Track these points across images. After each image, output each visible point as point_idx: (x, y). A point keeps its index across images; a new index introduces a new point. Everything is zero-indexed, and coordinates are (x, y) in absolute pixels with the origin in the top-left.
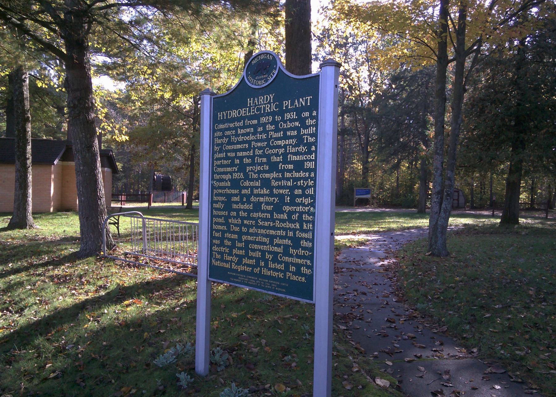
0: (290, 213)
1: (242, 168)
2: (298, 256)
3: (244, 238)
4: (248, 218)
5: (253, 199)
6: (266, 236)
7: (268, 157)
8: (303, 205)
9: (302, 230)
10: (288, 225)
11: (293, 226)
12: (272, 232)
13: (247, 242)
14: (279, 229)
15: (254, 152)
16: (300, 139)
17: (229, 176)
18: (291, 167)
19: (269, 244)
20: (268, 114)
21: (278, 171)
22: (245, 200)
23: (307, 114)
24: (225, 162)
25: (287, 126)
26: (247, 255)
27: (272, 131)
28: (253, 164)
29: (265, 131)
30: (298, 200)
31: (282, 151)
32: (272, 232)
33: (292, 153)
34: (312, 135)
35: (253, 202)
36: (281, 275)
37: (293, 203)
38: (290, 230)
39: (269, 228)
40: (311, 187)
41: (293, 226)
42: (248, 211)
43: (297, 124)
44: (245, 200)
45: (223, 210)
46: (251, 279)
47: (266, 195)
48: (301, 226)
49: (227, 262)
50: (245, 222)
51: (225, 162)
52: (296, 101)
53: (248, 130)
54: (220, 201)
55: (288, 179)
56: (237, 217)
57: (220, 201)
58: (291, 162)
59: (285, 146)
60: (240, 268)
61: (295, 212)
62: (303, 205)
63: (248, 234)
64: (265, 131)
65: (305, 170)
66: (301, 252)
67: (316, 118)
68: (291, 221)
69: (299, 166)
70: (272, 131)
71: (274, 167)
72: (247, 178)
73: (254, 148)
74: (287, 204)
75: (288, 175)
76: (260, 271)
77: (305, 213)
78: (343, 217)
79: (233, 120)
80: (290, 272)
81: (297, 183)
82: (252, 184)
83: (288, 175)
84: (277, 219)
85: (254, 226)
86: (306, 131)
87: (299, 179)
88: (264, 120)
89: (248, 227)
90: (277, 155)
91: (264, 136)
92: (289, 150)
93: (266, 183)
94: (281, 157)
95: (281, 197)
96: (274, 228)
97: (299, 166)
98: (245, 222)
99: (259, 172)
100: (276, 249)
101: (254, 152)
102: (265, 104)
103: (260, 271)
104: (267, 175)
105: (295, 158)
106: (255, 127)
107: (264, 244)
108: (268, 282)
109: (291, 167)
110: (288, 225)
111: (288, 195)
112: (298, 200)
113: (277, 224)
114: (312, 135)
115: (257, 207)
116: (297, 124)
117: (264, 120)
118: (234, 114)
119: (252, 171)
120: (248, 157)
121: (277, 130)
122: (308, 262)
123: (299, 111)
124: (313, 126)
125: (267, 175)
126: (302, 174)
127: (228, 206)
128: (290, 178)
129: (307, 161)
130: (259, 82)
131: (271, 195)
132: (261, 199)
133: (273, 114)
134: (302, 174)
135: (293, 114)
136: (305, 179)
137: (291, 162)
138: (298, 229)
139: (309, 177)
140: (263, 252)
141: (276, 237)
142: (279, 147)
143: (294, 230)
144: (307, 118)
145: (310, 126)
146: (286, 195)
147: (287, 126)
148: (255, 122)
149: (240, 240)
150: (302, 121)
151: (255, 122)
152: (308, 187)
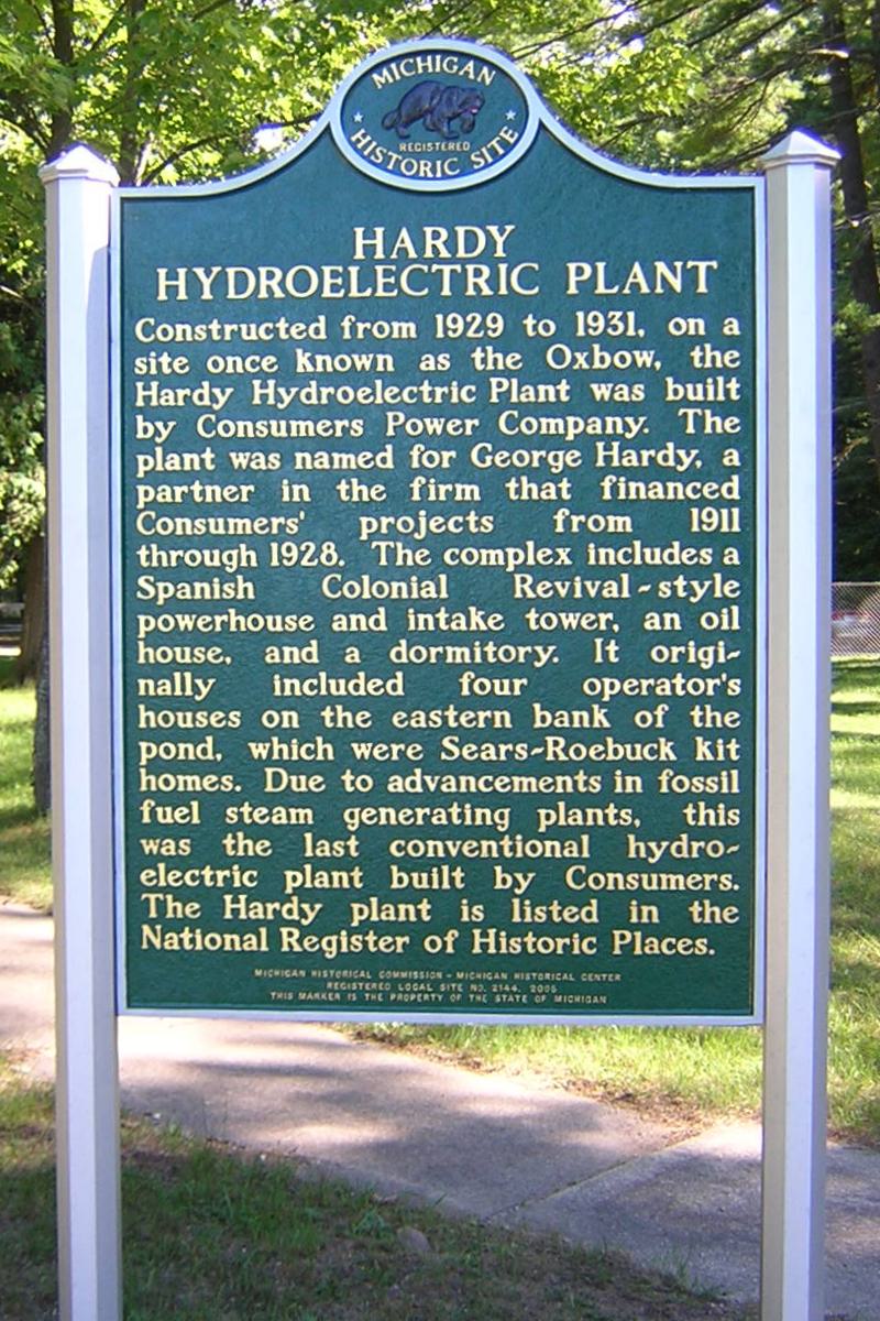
0: (621, 708)
1: (327, 516)
2: (669, 864)
3: (355, 818)
4: (381, 732)
5: (402, 652)
6: (493, 800)
7: (493, 482)
8: (692, 670)
9: (687, 764)
10: (614, 750)
11: (643, 752)
12: (525, 784)
13: (374, 838)
14: (569, 768)
15: (402, 457)
16: (664, 422)
17: (246, 555)
18: (622, 523)
19: (512, 833)
20: (484, 305)
21: (547, 539)
22: (353, 656)
23: (695, 325)
24: (215, 493)
25: (589, 359)
26: (377, 885)
27: (507, 373)
28: (398, 501)
29: (462, 370)
30: (661, 654)
31: (570, 458)
32: (525, 784)
33: (621, 471)
34: (723, 409)
35: (408, 668)
36: (583, 946)
37: (635, 663)
38: (629, 767)
39: (510, 767)
40: (726, 602)
41: (643, 752)
42: (381, 707)
43: (645, 358)
44: (353, 656)
45: (209, 705)
46: (404, 981)
47: (485, 637)
48: (685, 749)
49: (243, 927)
50: (361, 750)
51: (215, 493)
52: (637, 268)
53: (363, 362)
54: (183, 668)
55: (611, 572)
56: (309, 730)
57: (183, 668)
58: (617, 506)
59: (585, 443)
60: (330, 946)
61: (651, 701)
62: (692, 670)
63: (379, 797)
64: (462, 370)
65: (700, 540)
66: (685, 847)
67: (746, 344)
68: (624, 730)
69: (663, 522)
70: (507, 373)
71: (525, 523)
72: (358, 559)
73: (403, 443)
74: (606, 669)
75: (609, 556)
76: (464, 942)
77: (703, 700)
78: (343, 1087)
79: (267, 310)
80: (633, 928)
81: (656, 589)
82: (396, 589)
83: (609, 556)
84: (552, 730)
85: (417, 764)
86: (694, 392)
87: (669, 572)
88: (451, 325)
89: (381, 770)
90: (540, 474)
91: (462, 394)
92: (608, 459)
93: (473, 588)
94: (565, 485)
95: (575, 646)
96: (537, 767)
97: (663, 522)
98: (361, 750)
99: (437, 543)
100: (550, 848)
101: (402, 457)
102: (464, 262)
103: (464, 942)
104: (492, 557)
105: (637, 490)
106: (409, 356)
107: (491, 832)
108: (511, 981)
109: (622, 523)
110: (614, 750)
111: (607, 636)
112: (661, 654)
113: (554, 748)
114: (723, 409)
115: (433, 685)
116: (645, 358)
117: (451, 325)
118: (270, 282)
119: (393, 534)
120: (369, 476)
121: (535, 372)
122: (726, 882)
123: (655, 310)
124: (727, 373)
125: (492, 557)
126: (679, 555)
127: (243, 679)
128: (620, 568)
129: (702, 503)
130: (424, 168)
131: (516, 633)
132: (457, 654)
133: (513, 307)
134: (679, 555)
135: (624, 319)
136: (696, 572)
137: (617, 506)
138: (668, 764)
139: (718, 565)
140: (478, 871)
141: (550, 801)
142: (556, 442)
143: (649, 770)
144: (698, 340)
145: (714, 372)
146: (598, 633)
147: (589, 359)
148: (407, 329)
149: (328, 827)
150: (676, 356)
151: (407, 329)
152: (714, 603)
